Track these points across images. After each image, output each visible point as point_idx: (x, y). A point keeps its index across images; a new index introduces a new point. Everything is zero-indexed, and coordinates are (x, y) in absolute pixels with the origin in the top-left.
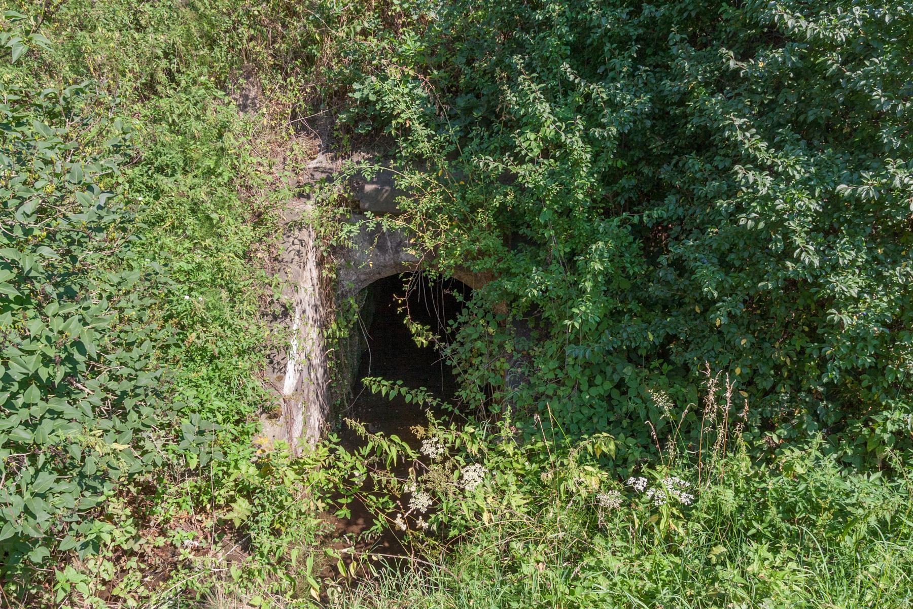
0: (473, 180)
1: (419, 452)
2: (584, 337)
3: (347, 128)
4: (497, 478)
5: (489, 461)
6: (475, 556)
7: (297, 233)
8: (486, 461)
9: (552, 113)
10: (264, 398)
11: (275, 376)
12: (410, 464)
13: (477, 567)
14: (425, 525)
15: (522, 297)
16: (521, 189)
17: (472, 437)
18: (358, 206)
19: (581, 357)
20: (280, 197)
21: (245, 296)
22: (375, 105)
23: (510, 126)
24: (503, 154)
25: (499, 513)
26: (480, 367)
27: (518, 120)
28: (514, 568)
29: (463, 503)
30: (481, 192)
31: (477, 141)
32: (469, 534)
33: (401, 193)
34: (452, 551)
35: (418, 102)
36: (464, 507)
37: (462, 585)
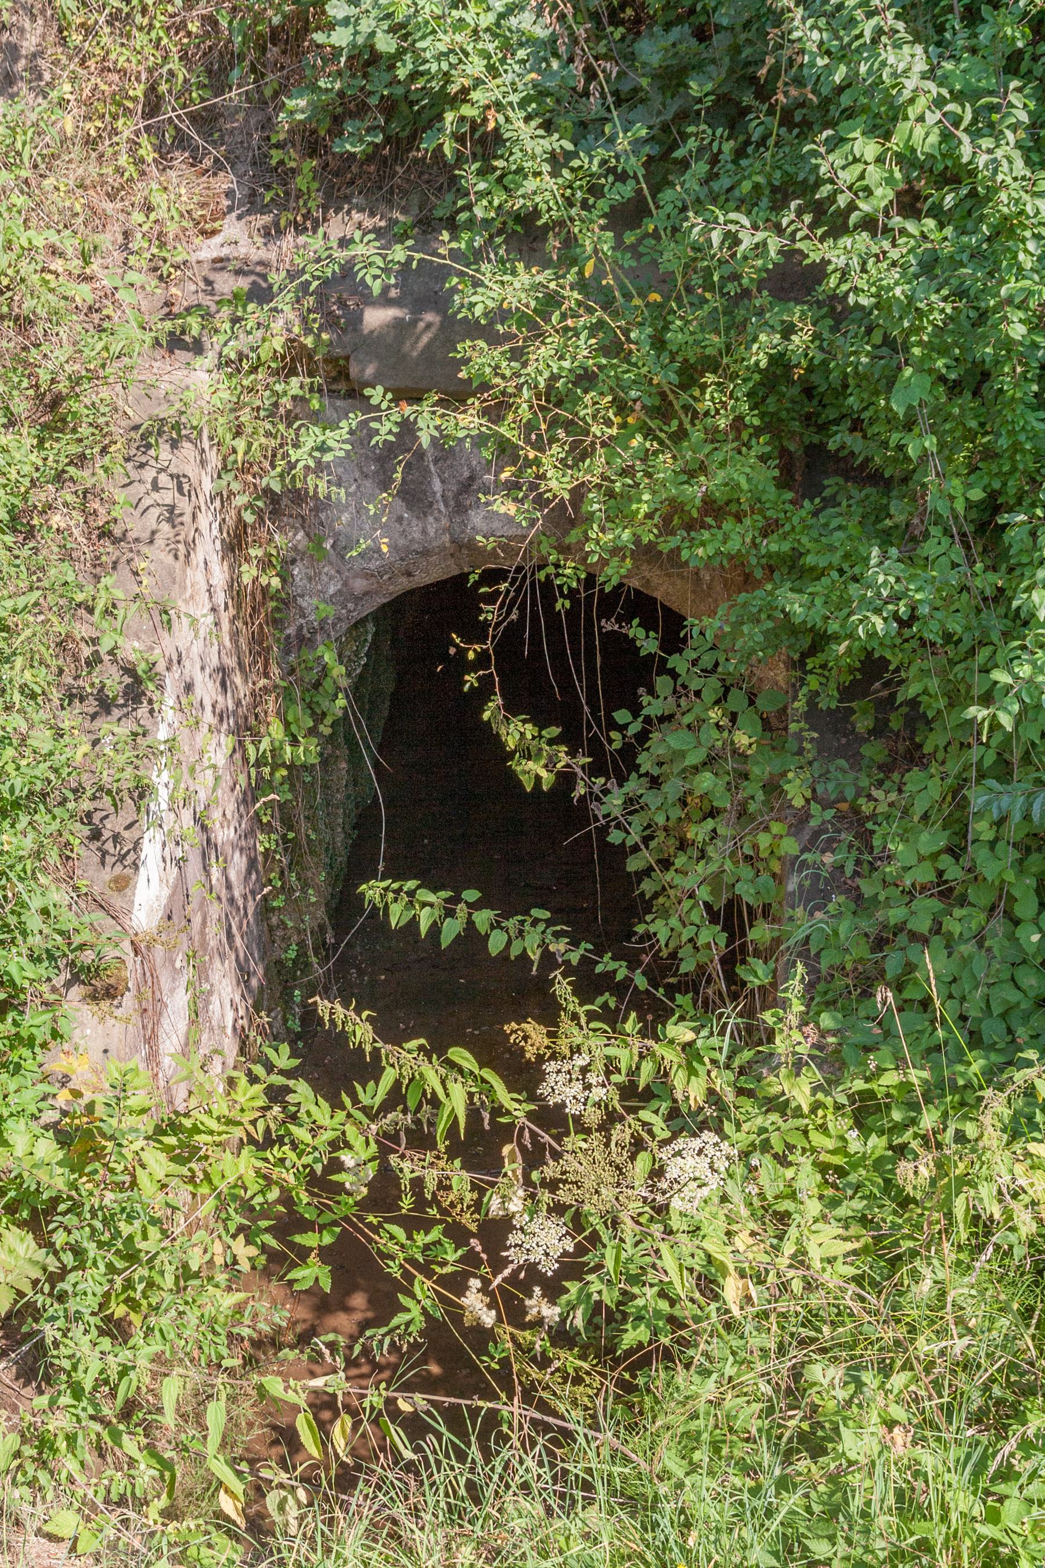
0: (689, 290)
1: (532, 1098)
2: (1026, 759)
3: (310, 141)
4: (764, 1177)
5: (738, 1126)
6: (702, 1407)
7: (164, 452)
8: (728, 1127)
9: (930, 74)
10: (77, 940)
11: (107, 875)
12: (505, 1133)
13: (705, 1436)
14: (551, 1313)
15: (836, 638)
16: (837, 312)
17: (690, 1056)
18: (343, 374)
19: (1017, 816)
20: (115, 348)
21: (17, 643)
22: (392, 67)
23: (800, 122)
24: (778, 206)
25: (771, 1278)
26: (710, 850)
27: (826, 103)
28: (814, 1442)
29: (664, 1248)
30: (711, 323)
31: (700, 168)
32: (682, 1342)
33: (474, 329)
34: (629, 1388)
35: (521, 54)
36: (669, 1261)
37: (663, 1489)
